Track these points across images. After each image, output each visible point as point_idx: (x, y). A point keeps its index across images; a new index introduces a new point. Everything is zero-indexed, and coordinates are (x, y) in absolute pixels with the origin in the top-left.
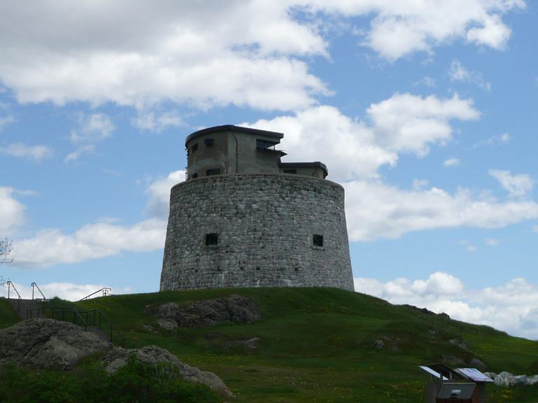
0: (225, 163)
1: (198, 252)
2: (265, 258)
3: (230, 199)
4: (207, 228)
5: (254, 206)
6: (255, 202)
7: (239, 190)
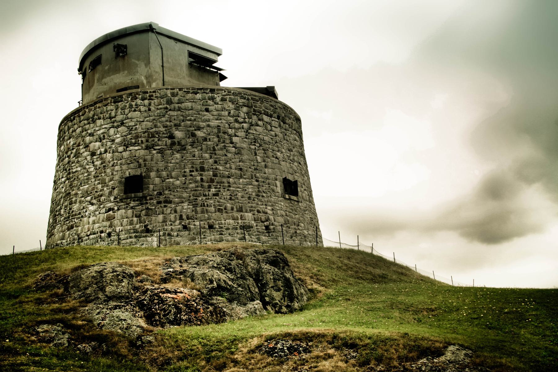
0: (147, 78)
1: (109, 205)
2: (220, 210)
3: (159, 124)
4: (124, 167)
5: (199, 134)
6: (199, 128)
7: (174, 110)
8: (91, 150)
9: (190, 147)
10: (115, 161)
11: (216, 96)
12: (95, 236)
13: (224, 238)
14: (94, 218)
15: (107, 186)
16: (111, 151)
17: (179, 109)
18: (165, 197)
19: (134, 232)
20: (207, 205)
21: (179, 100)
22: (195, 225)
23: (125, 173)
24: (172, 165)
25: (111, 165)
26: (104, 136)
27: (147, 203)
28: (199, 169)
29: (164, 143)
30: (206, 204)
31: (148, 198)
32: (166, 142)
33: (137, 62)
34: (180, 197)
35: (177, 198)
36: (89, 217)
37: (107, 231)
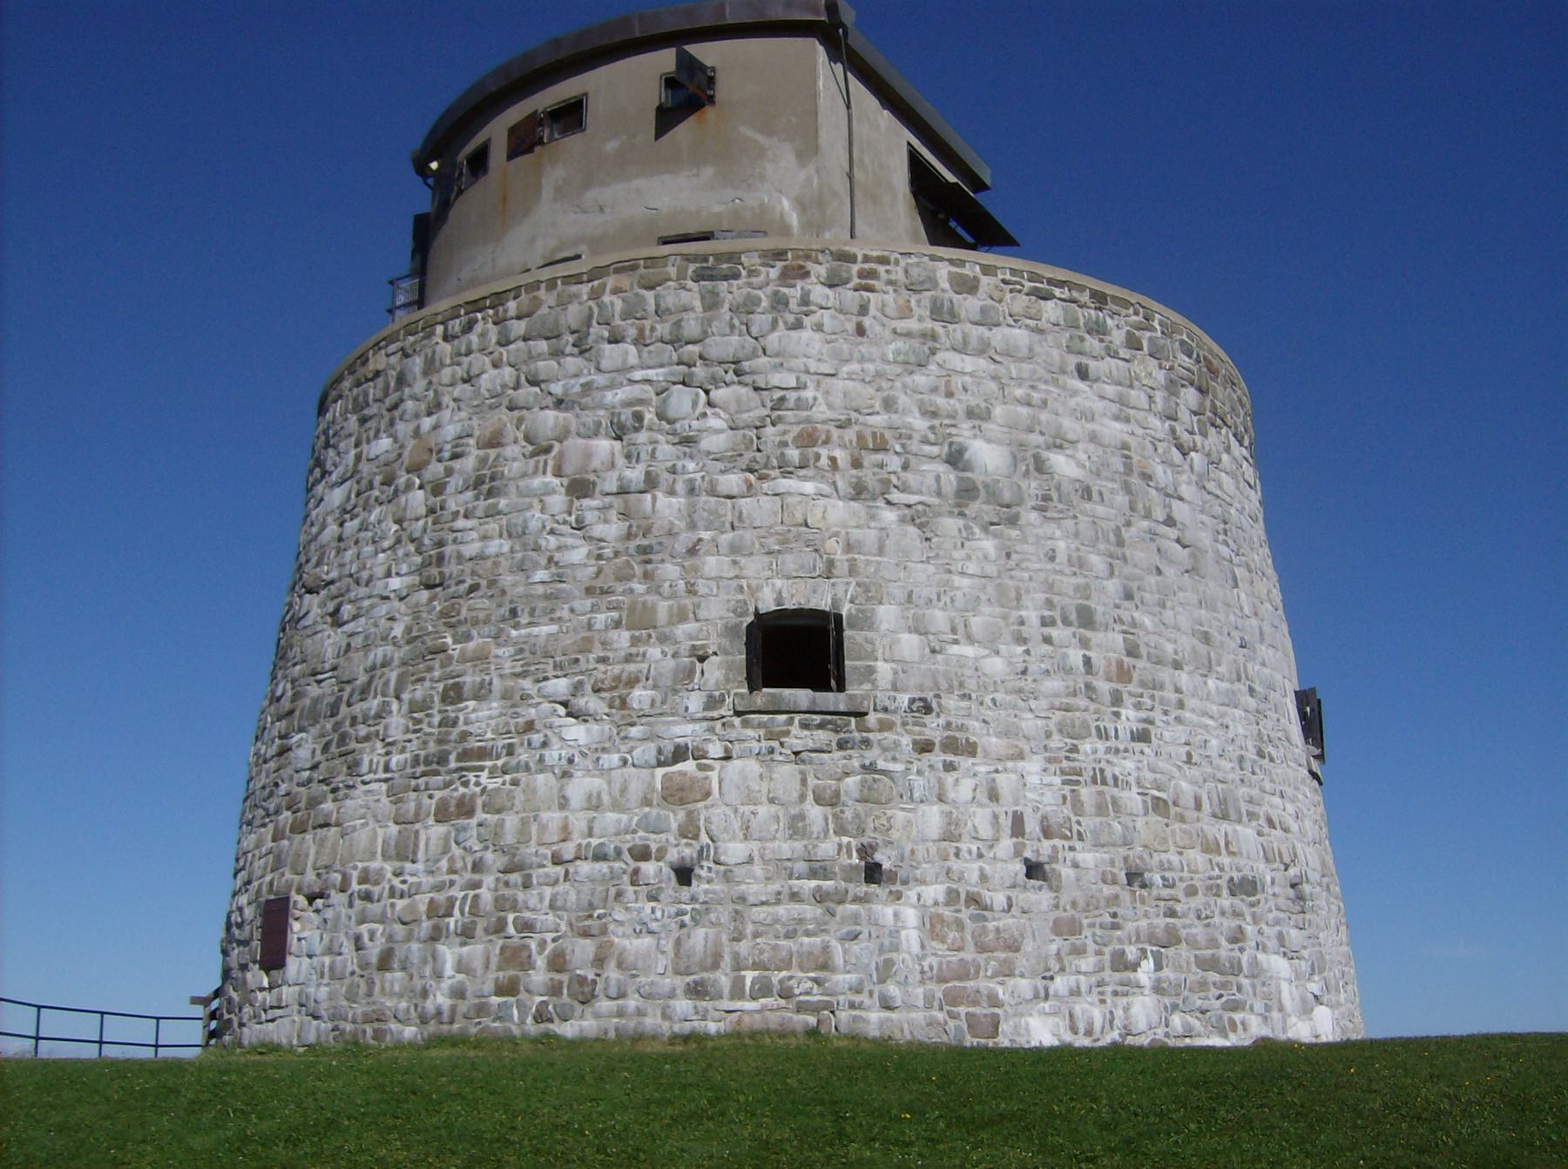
0: (802, 205)
1: (684, 732)
2: (1159, 806)
3: (903, 400)
4: (754, 566)
5: (1062, 465)
6: (1060, 443)
7: (962, 349)
8: (569, 469)
9: (1034, 516)
10: (706, 535)
11: (1109, 321)
12: (603, 867)
13: (1183, 933)
14: (597, 783)
15: (663, 639)
16: (680, 487)
17: (983, 350)
18: (948, 725)
19: (813, 874)
20: (1115, 778)
21: (984, 310)
22: (1076, 866)
23: (754, 591)
24: (966, 582)
25: (681, 546)
26: (639, 417)
27: (866, 743)
28: (1073, 617)
29: (930, 481)
30: (1109, 775)
31: (872, 719)
32: (938, 478)
33: (760, 138)
34: (1008, 733)
35: (998, 735)
36: (566, 775)
37: (673, 855)
